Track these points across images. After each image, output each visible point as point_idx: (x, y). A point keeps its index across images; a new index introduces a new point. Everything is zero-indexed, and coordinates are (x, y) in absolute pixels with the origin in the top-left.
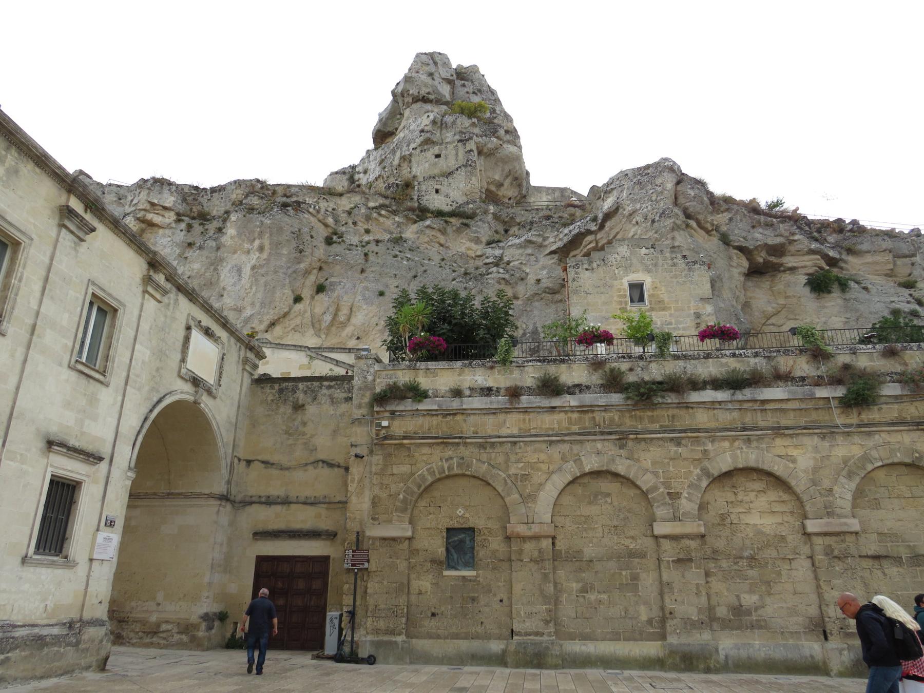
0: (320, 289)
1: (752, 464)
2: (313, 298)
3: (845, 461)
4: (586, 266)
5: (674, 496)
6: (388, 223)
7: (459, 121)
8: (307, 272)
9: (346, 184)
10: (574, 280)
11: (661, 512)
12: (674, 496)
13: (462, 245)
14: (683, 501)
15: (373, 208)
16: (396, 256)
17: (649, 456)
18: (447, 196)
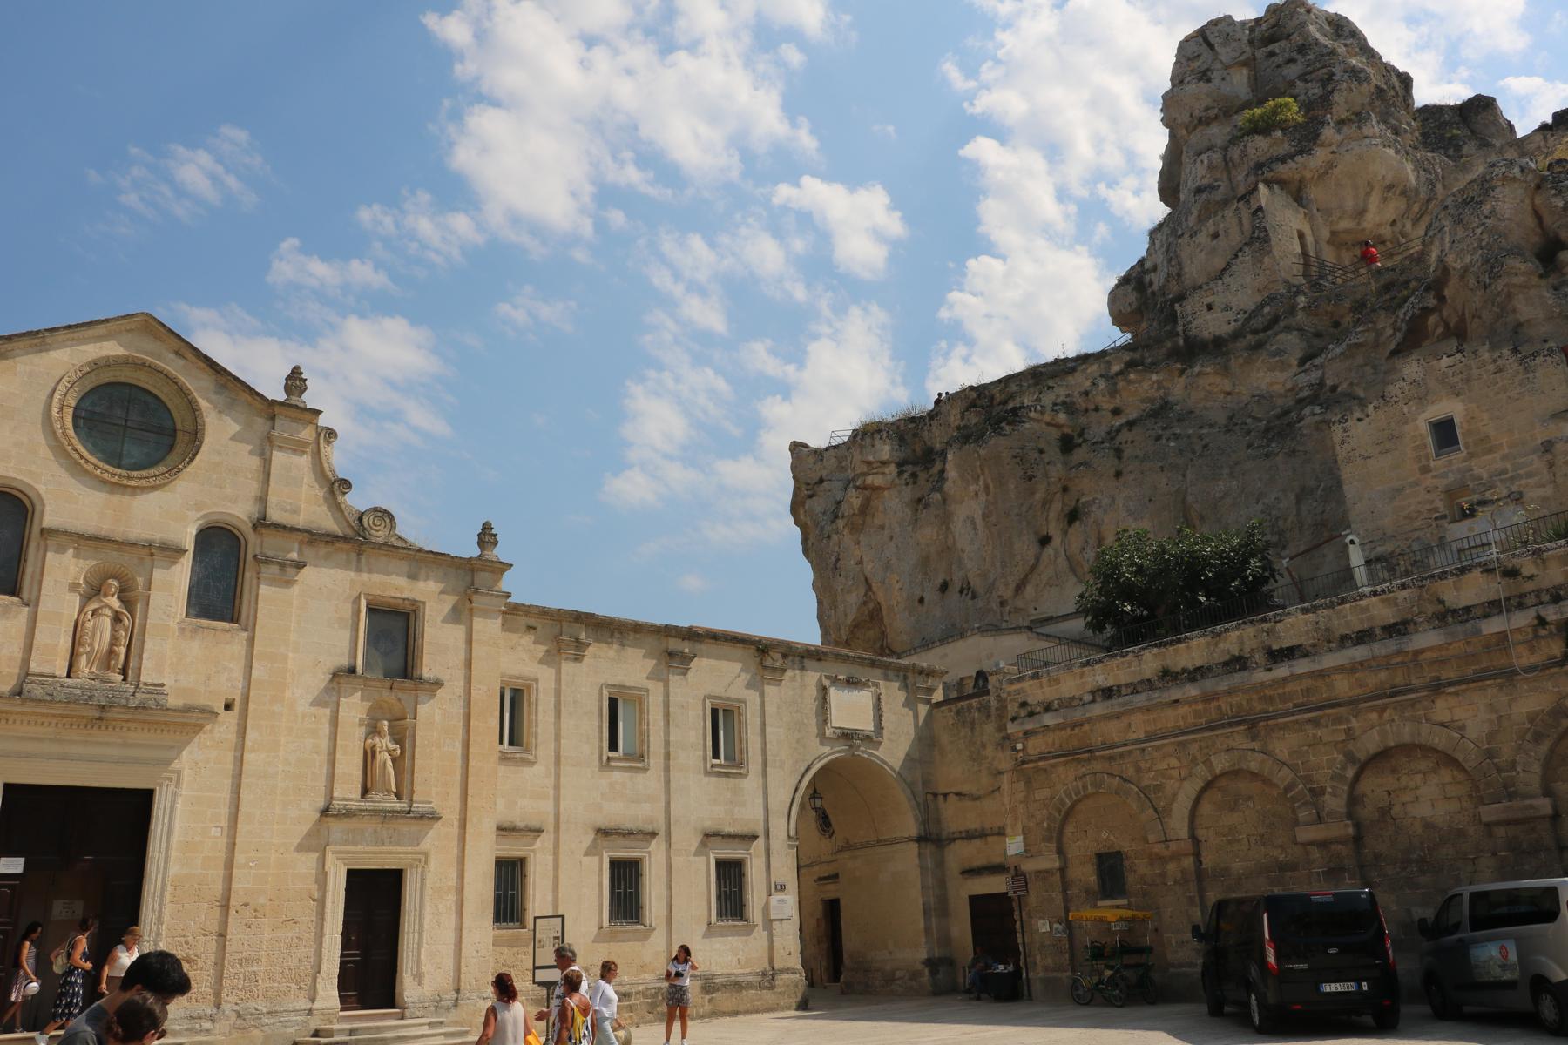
0: (1073, 516)
1: (1407, 739)
2: (1065, 533)
3: (1532, 718)
4: (1357, 414)
5: (1317, 793)
7: (1250, 150)
8: (1046, 503)
10: (1343, 442)
11: (1303, 815)
12: (1317, 793)
14: (1327, 797)
15: (1118, 374)
16: (1159, 438)
17: (1283, 746)
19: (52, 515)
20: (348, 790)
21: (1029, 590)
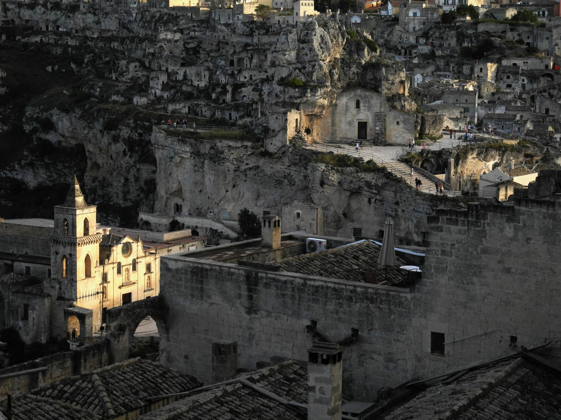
0: (234, 186)
6: (254, 160)
9: (258, 97)
13: (279, 167)
18: (275, 145)
19: (122, 264)
20: (146, 288)
21: (222, 202)
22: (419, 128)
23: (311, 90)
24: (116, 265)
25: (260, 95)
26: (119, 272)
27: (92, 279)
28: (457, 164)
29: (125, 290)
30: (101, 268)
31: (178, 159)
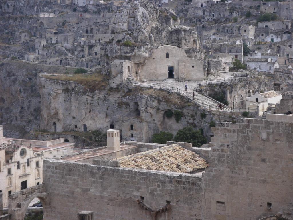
7: (124, 49)
18: (116, 83)
19: (21, 162)
22: (206, 69)
23: (138, 47)
24: (16, 164)
25: (106, 52)
26: (18, 168)
27: (1, 173)
28: (231, 92)
29: (23, 180)
30: (8, 167)
31: (55, 94)
